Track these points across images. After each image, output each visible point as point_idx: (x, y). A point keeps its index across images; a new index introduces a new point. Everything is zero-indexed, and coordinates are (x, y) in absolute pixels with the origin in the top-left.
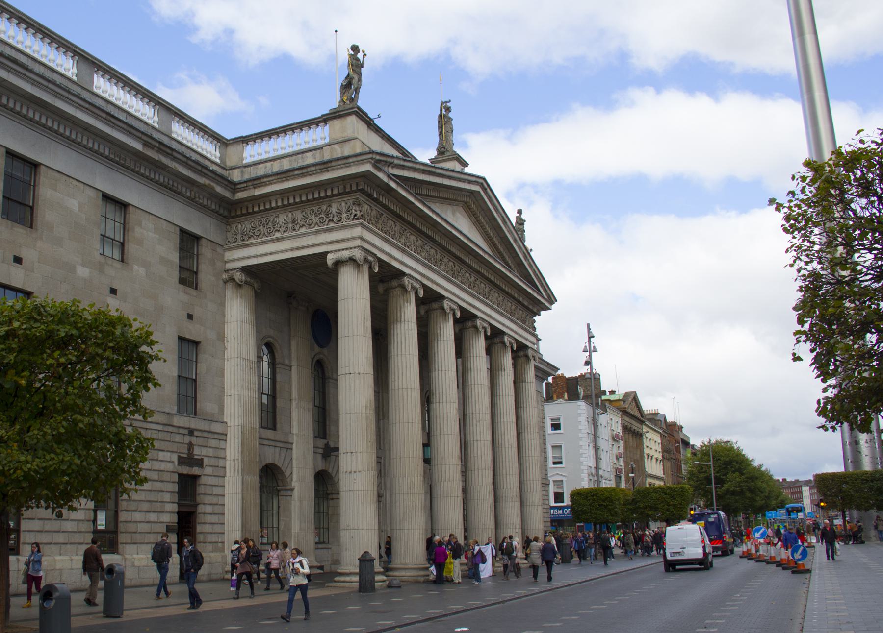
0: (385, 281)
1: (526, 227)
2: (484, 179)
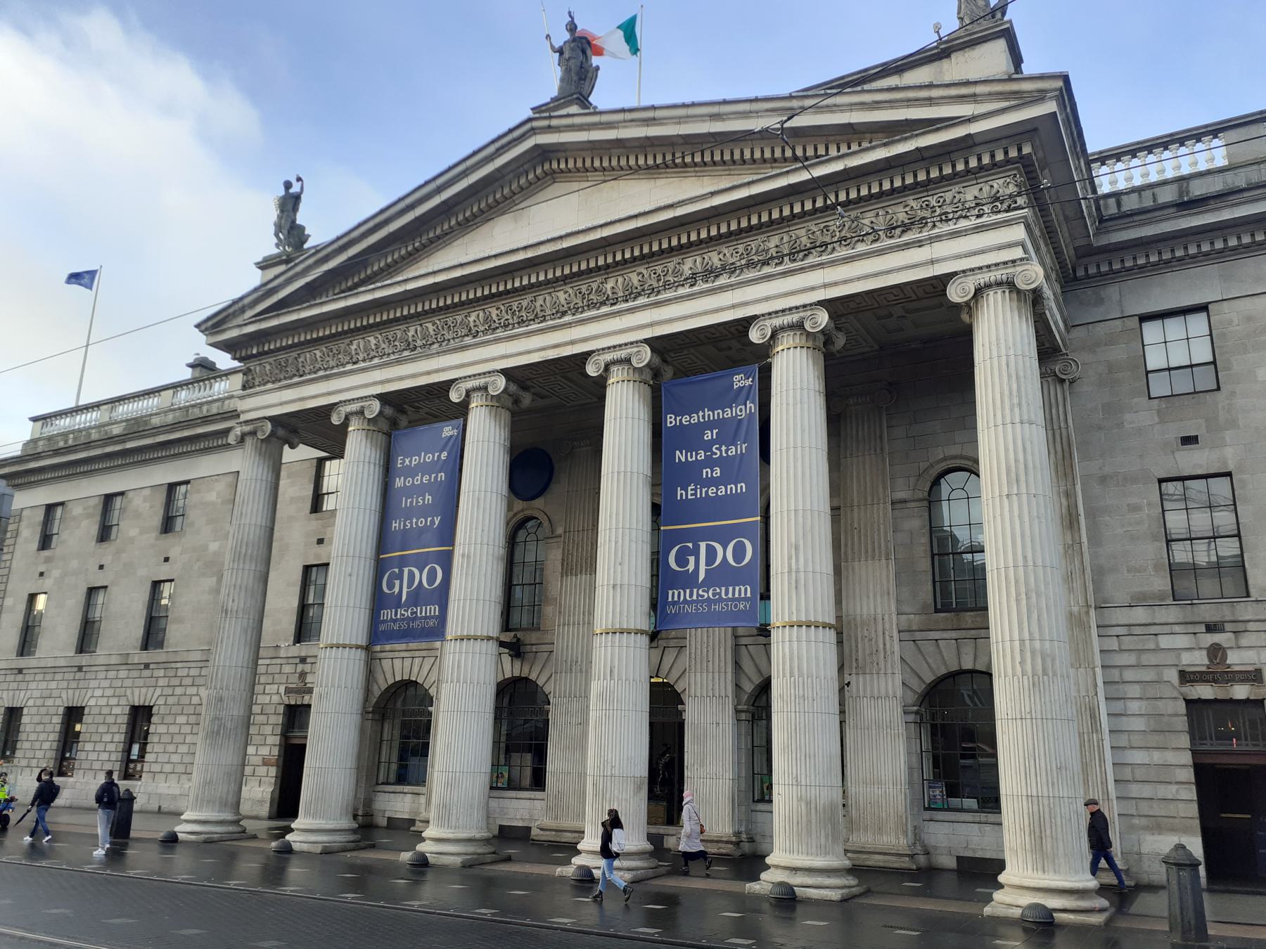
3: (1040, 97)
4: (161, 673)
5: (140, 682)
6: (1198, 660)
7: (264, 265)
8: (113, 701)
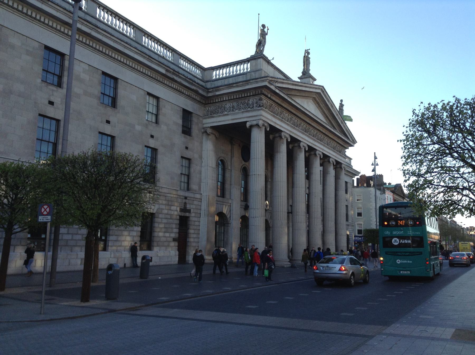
0: (272, 134)
1: (344, 108)
2: (323, 87)
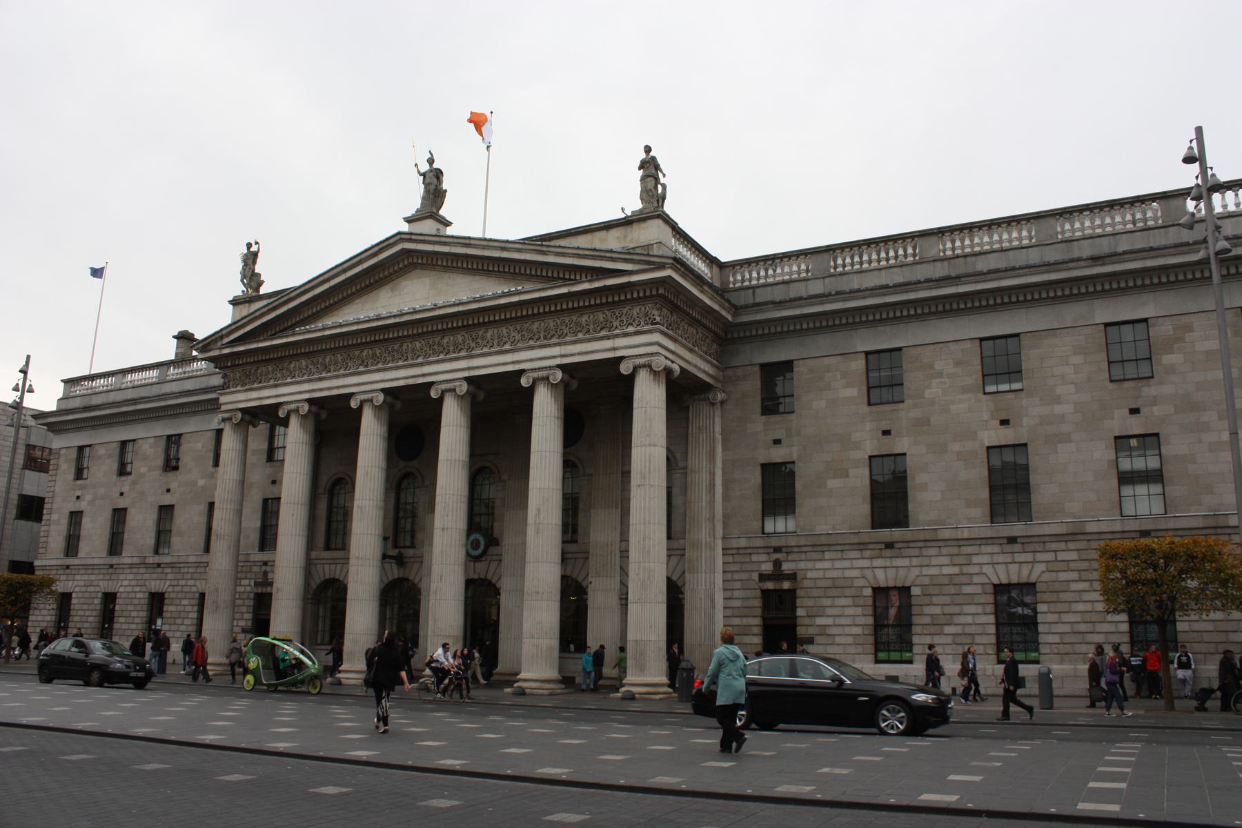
2: (399, 233)
3: (661, 267)
4: (169, 570)
5: (154, 576)
6: (767, 567)
7: (235, 302)
8: (137, 589)
